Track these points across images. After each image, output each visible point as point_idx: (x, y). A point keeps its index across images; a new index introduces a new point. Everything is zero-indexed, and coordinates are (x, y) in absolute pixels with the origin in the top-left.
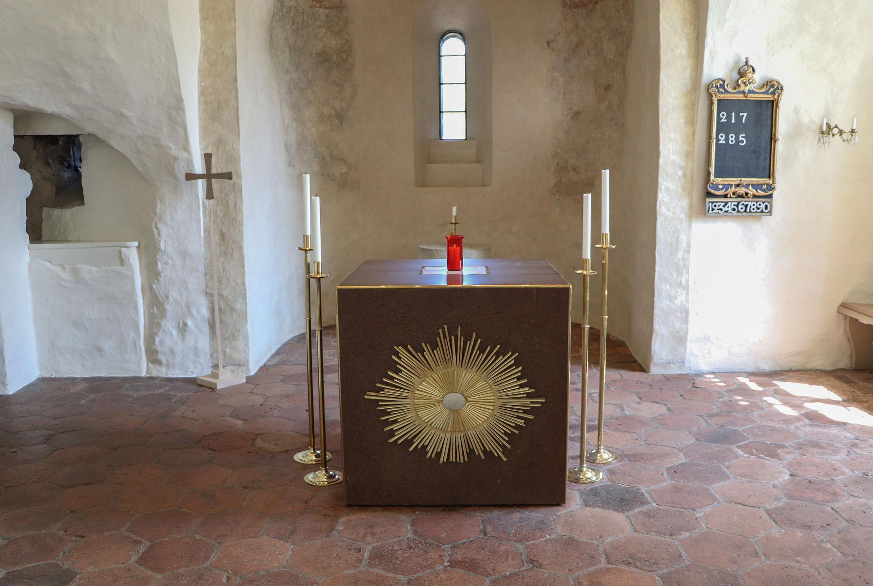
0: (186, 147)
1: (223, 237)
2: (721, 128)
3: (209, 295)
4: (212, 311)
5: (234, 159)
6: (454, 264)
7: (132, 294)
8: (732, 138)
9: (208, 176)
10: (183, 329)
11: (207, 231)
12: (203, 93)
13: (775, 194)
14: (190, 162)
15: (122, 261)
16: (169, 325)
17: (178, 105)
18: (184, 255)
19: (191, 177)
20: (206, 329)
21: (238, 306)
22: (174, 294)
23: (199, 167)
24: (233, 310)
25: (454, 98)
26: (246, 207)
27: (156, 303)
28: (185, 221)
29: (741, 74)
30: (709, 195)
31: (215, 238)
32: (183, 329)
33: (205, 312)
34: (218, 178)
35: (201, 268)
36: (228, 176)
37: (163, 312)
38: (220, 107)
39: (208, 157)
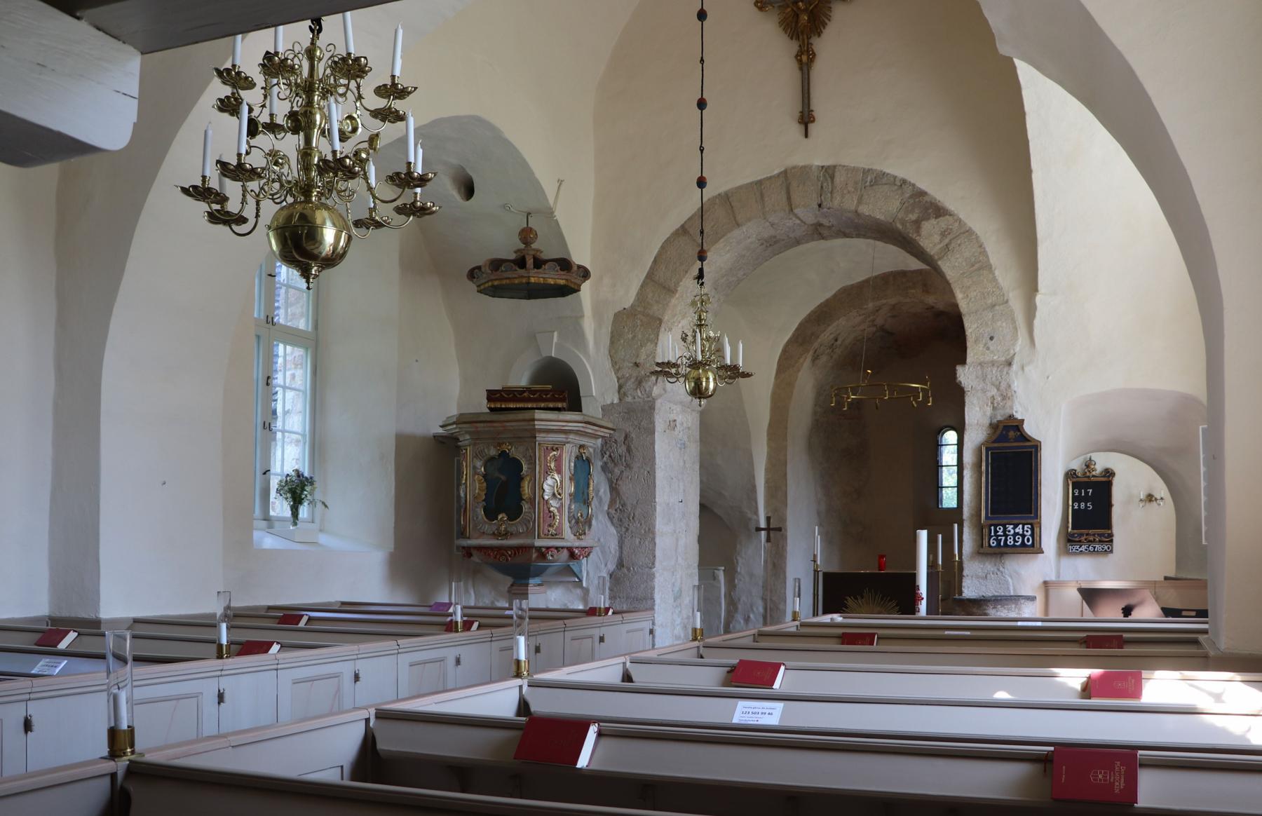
0: (756, 513)
1: (774, 565)
2: (1075, 499)
3: (764, 600)
4: (765, 609)
5: (783, 519)
6: (881, 567)
7: (719, 597)
8: (1083, 505)
9: (768, 529)
10: (747, 620)
11: (766, 562)
12: (767, 482)
13: (1115, 539)
14: (758, 521)
15: (715, 578)
16: (739, 617)
17: (753, 489)
18: (751, 575)
19: (759, 529)
20: (761, 620)
21: (781, 607)
22: (744, 598)
23: (763, 524)
24: (778, 608)
25: (949, 478)
26: (789, 548)
27: (732, 604)
28: (753, 556)
29: (1088, 466)
30: (1069, 541)
31: (770, 566)
32: (747, 620)
33: (761, 610)
34: (775, 531)
35: (761, 583)
36: (780, 529)
37: (736, 609)
38: (777, 489)
39: (768, 519)
